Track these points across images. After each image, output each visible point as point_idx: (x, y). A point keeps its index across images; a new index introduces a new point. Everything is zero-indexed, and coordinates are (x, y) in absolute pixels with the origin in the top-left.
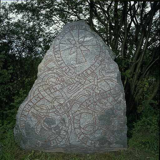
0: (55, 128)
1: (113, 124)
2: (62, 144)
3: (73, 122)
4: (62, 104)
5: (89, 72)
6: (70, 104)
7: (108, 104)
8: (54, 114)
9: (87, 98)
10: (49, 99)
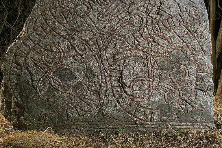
0: (76, 87)
1: (186, 78)
3: (110, 75)
7: (177, 40)
9: (135, 29)
10: (64, 33)
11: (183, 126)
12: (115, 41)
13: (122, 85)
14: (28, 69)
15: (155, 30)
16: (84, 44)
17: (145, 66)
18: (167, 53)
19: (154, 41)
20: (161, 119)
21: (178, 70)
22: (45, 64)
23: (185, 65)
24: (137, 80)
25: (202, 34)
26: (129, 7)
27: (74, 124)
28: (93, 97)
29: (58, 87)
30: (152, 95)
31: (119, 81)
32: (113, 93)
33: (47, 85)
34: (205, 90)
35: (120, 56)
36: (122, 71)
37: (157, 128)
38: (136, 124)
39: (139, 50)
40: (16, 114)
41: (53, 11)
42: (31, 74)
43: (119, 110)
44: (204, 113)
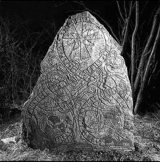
0: (60, 126)
1: (119, 122)
5: (94, 68)
7: (114, 101)
11: (117, 148)
12: (80, 102)
13: (85, 126)
14: (35, 116)
15: (102, 96)
17: (96, 116)
18: (108, 109)
19: (101, 102)
20: (105, 144)
21: (114, 118)
22: (44, 114)
23: (118, 115)
24: (92, 123)
25: (127, 98)
26: (88, 83)
27: (59, 146)
28: (69, 131)
30: (100, 131)
31: (83, 123)
32: (80, 130)
33: (45, 125)
34: (129, 129)
35: (84, 110)
36: (84, 118)
37: (103, 149)
38: (92, 147)
39: (93, 107)
40: (29, 139)
41: (47, 85)
42: (37, 119)
43: (83, 139)
44: (129, 142)
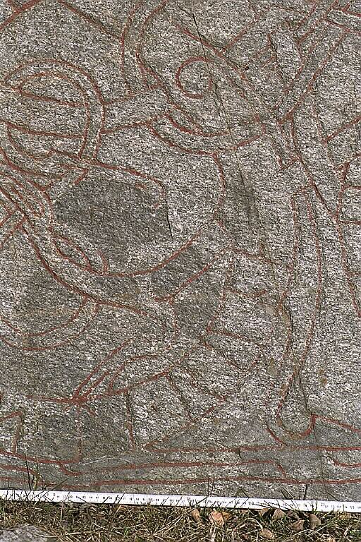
2: (237, 414)
4: (227, 46)
6: (299, 41)
8: (151, 143)
16: (208, 59)
29: (79, 277)
